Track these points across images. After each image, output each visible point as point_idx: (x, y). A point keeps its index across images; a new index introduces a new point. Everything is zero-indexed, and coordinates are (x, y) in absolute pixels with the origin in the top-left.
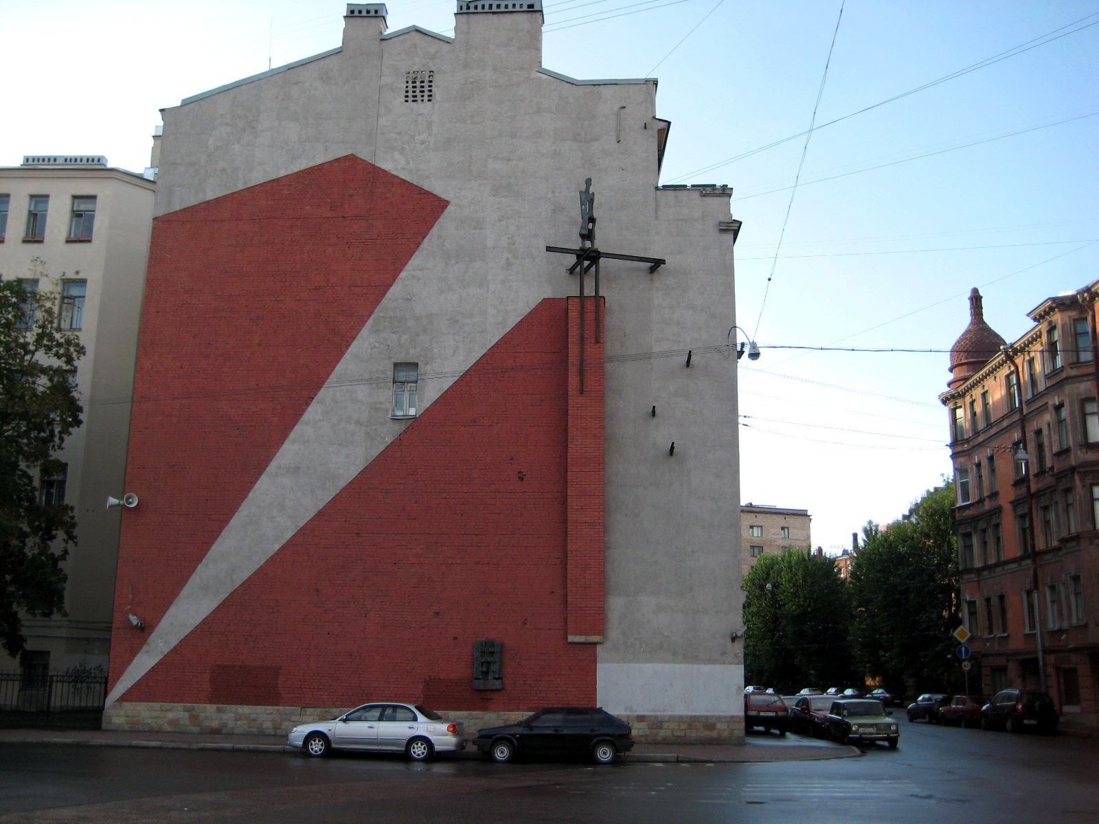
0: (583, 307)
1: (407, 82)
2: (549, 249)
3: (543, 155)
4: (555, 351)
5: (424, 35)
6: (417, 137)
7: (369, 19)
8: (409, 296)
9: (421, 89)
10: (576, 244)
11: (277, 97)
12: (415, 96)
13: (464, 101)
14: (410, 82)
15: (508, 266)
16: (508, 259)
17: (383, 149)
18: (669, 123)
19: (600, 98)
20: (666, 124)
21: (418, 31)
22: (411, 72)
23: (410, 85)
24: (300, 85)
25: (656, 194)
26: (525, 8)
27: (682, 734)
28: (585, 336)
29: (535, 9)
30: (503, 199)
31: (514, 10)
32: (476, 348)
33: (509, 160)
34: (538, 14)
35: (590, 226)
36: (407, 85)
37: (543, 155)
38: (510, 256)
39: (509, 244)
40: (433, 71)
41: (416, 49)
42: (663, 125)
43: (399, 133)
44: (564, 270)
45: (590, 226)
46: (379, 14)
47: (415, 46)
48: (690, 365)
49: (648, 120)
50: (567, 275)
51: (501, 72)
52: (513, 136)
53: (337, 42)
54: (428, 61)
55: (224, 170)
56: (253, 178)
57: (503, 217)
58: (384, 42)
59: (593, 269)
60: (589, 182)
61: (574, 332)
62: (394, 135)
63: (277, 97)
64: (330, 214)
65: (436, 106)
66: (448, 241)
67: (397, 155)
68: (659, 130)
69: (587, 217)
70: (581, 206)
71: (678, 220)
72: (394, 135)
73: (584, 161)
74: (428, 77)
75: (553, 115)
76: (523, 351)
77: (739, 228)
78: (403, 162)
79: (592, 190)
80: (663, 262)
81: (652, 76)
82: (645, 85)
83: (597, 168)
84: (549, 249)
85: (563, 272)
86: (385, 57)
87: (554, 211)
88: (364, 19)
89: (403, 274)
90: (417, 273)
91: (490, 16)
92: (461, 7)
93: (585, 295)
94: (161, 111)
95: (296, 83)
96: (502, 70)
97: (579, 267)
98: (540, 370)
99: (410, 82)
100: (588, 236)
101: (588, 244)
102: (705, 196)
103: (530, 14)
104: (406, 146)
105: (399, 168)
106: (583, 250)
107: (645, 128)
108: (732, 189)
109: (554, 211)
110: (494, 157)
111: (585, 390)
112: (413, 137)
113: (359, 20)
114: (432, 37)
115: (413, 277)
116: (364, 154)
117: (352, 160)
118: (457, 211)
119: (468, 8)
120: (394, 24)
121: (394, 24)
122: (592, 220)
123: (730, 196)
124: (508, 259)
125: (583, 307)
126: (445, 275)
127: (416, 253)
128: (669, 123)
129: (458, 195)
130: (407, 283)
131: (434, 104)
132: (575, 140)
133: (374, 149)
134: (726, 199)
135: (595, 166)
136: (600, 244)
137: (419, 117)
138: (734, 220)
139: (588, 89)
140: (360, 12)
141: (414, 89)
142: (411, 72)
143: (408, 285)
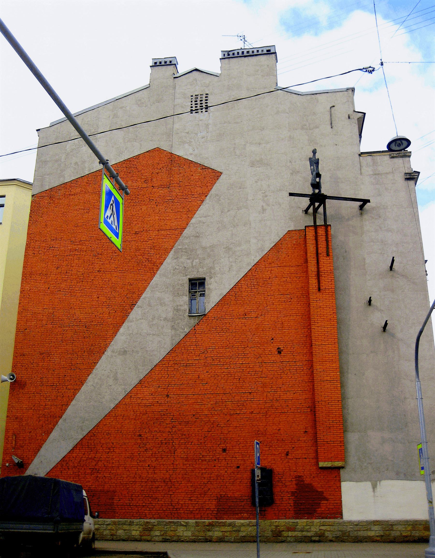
0: (316, 232)
1: (192, 102)
2: (291, 194)
3: (282, 140)
4: (299, 265)
5: (201, 73)
6: (199, 134)
7: (166, 66)
8: (197, 234)
9: (201, 105)
10: (309, 191)
11: (109, 117)
12: (196, 104)
13: (229, 110)
14: (193, 101)
15: (263, 211)
16: (263, 206)
17: (177, 143)
18: (365, 114)
19: (318, 102)
20: (363, 114)
21: (196, 70)
22: (194, 95)
23: (194, 103)
24: (124, 108)
25: (359, 158)
26: (265, 52)
27: (409, 533)
28: (319, 252)
29: (272, 51)
30: (258, 168)
31: (258, 53)
32: (245, 266)
33: (260, 144)
34: (274, 55)
35: (318, 180)
36: (192, 103)
37: (282, 140)
38: (264, 204)
39: (263, 197)
40: (208, 94)
41: (196, 81)
42: (361, 115)
43: (188, 133)
44: (301, 211)
45: (318, 180)
46: (173, 63)
47: (196, 80)
48: (393, 269)
49: (351, 112)
50: (304, 214)
51: (252, 91)
52: (263, 129)
53: (146, 82)
54: (205, 88)
55: (76, 163)
56: (94, 166)
57: (258, 180)
58: (176, 79)
59: (322, 208)
60: (314, 152)
61: (311, 248)
62: (184, 134)
63: (109, 117)
64: (145, 185)
65: (211, 114)
66: (222, 197)
67: (186, 146)
68: (358, 118)
69: (314, 173)
70: (311, 167)
71: (376, 174)
72: (184, 134)
73: (310, 141)
74: (205, 97)
75: (287, 114)
76: (277, 266)
77: (419, 174)
78: (191, 151)
79: (317, 156)
80: (368, 201)
81: (351, 86)
82: (346, 92)
83: (319, 145)
84: (291, 194)
85: (300, 213)
86: (177, 88)
87: (292, 174)
88: (163, 67)
89: (193, 221)
90: (203, 219)
91: (243, 58)
92: (224, 55)
93: (318, 224)
94: (37, 130)
95: (121, 108)
96: (252, 90)
97: (312, 207)
98: (289, 278)
99: (193, 101)
100: (316, 185)
101: (317, 191)
102: (393, 157)
103: (269, 55)
104: (193, 140)
105: (188, 154)
106: (314, 194)
107: (349, 118)
108: (411, 152)
109: (292, 174)
110: (250, 143)
111: (322, 288)
112: (196, 134)
113: (160, 67)
114: (207, 73)
115: (200, 221)
116: (165, 147)
117: (158, 150)
118: (227, 179)
119: (229, 55)
120: (182, 69)
121: (182, 69)
122: (318, 175)
123: (409, 156)
124: (263, 206)
125: (316, 232)
126: (222, 219)
127: (201, 206)
128: (365, 114)
129: (227, 168)
130: (196, 225)
131: (209, 114)
132: (302, 128)
133: (171, 143)
134: (407, 159)
135: (318, 144)
136: (324, 191)
137: (200, 122)
138: (414, 171)
139: (309, 97)
140: (160, 63)
141: (196, 106)
142: (194, 95)
143: (197, 227)
